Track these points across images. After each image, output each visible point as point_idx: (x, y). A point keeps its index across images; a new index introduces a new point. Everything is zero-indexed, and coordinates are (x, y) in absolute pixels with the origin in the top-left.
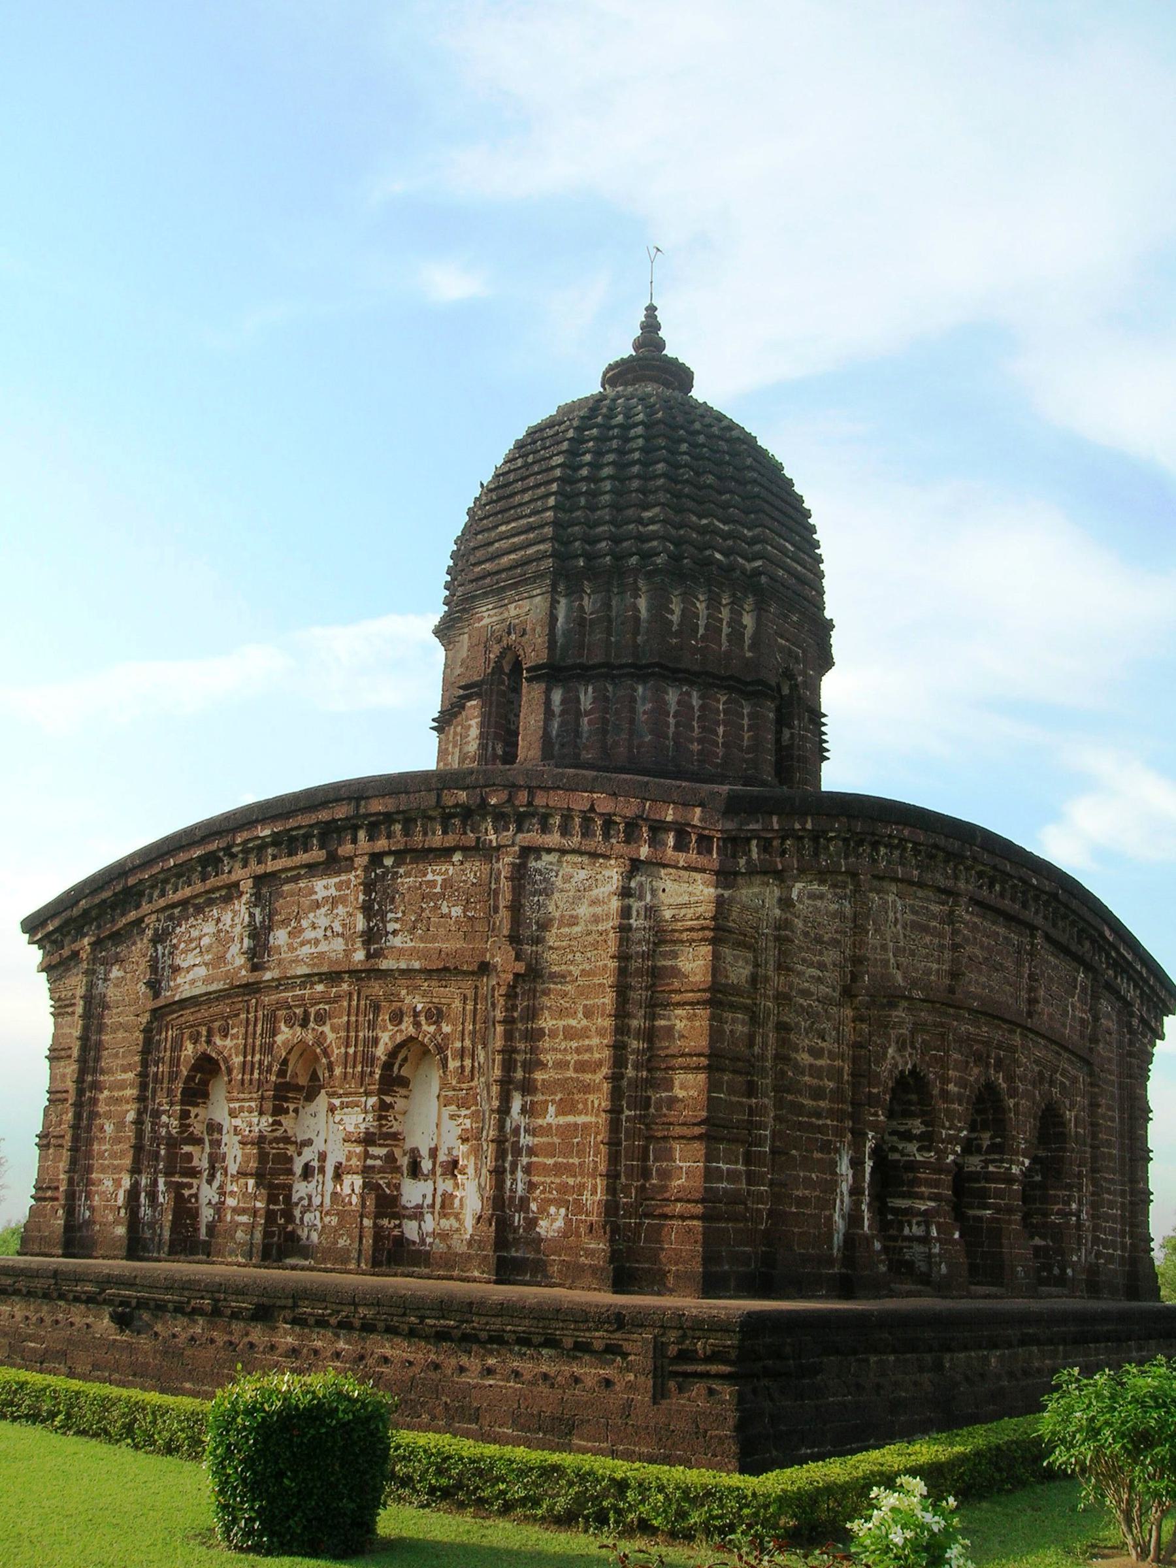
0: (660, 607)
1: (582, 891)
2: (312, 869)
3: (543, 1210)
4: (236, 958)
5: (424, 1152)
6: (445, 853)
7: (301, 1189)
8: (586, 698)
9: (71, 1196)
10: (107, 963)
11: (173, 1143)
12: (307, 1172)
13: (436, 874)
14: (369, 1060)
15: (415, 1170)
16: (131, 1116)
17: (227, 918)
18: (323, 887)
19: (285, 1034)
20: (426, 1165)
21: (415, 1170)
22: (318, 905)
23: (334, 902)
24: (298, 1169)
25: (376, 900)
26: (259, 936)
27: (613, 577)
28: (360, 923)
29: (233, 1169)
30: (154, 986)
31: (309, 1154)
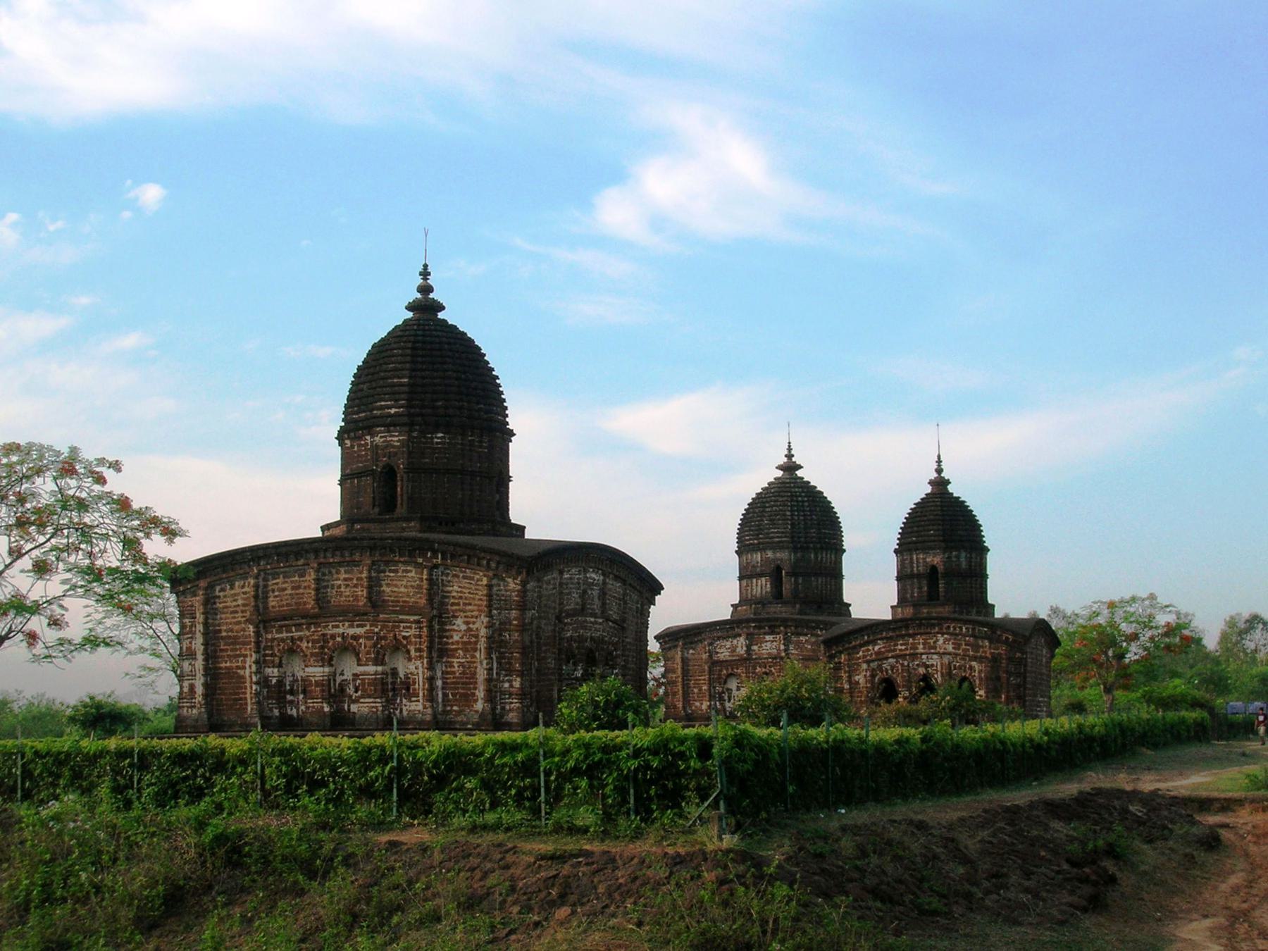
0: (816, 557)
4: (741, 651)
8: (800, 580)
9: (684, 708)
10: (688, 649)
11: (720, 694)
13: (803, 638)
16: (705, 687)
18: (768, 638)
19: (758, 669)
25: (787, 642)
26: (748, 647)
27: (805, 549)
28: (782, 647)
30: (710, 656)
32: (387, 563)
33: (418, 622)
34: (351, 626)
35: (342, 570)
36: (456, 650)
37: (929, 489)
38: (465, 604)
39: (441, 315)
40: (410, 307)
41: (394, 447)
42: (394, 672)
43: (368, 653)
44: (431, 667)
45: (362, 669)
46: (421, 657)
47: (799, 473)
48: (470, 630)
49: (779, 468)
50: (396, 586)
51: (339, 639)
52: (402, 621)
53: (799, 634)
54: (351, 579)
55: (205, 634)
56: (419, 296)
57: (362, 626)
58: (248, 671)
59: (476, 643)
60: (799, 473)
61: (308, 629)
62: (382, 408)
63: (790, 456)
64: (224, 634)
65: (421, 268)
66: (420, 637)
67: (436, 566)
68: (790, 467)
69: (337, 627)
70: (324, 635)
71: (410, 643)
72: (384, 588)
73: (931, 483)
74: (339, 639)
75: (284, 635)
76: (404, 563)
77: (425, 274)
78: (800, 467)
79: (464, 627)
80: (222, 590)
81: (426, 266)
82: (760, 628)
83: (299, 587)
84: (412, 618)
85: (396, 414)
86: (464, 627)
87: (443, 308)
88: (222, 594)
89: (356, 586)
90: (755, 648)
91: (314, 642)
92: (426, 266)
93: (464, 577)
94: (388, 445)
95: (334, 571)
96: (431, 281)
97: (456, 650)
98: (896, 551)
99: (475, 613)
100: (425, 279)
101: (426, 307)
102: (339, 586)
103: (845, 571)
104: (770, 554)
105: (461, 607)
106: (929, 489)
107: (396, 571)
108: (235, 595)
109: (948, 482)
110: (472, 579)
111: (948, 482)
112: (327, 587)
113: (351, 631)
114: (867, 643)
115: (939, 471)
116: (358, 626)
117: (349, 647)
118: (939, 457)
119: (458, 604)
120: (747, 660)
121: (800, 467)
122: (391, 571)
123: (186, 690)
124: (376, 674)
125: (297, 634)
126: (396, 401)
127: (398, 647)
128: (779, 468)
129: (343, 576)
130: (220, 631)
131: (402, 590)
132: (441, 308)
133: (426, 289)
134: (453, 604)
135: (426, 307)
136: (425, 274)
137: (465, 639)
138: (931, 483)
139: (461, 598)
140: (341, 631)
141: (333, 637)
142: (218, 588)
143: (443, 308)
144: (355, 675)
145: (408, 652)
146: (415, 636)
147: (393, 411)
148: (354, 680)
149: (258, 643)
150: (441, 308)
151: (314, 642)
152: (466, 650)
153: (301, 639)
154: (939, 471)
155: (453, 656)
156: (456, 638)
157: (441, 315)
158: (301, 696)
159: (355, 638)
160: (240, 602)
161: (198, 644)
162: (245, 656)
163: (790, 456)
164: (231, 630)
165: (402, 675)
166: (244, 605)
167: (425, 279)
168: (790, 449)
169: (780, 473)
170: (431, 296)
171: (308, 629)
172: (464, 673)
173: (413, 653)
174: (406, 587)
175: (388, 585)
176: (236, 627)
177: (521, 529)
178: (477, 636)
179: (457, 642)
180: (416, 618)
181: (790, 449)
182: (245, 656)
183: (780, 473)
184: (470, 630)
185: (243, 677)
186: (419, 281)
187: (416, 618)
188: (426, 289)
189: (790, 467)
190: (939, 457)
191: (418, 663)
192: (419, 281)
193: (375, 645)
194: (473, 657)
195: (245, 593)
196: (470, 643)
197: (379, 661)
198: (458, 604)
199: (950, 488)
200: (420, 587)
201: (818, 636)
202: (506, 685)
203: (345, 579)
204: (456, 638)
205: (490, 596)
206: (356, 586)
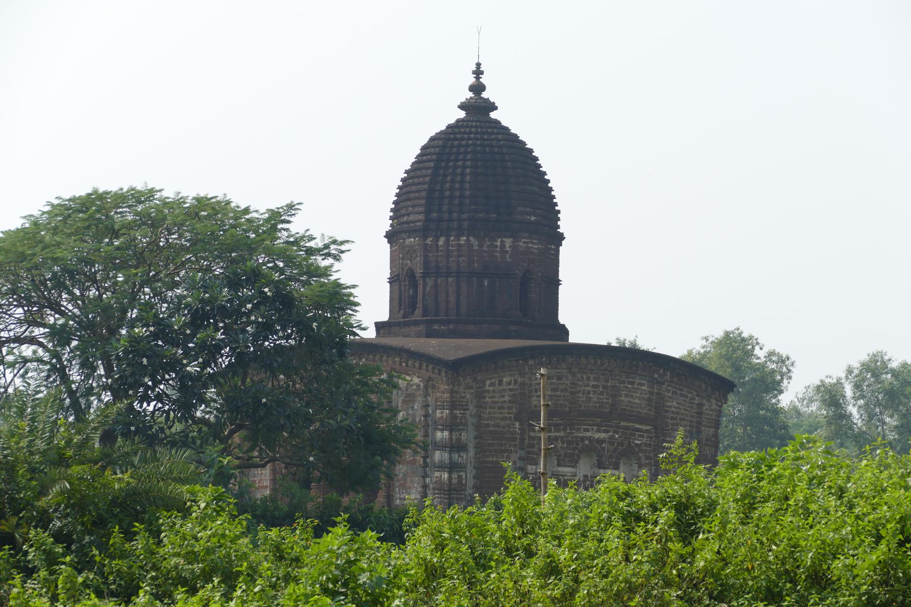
34: (598, 431)
35: (592, 376)
38: (681, 419)
39: (493, 115)
40: (462, 107)
43: (610, 457)
46: (650, 464)
50: (632, 397)
54: (597, 386)
55: (478, 427)
56: (471, 95)
57: (606, 431)
64: (492, 429)
65: (474, 68)
66: (650, 445)
69: (588, 430)
70: (576, 437)
74: (587, 442)
77: (478, 73)
80: (491, 385)
81: (478, 65)
83: (556, 390)
84: (644, 427)
87: (496, 108)
88: (491, 388)
89: (601, 393)
91: (569, 443)
92: (478, 65)
93: (681, 395)
95: (585, 377)
100: (478, 78)
101: (478, 107)
102: (589, 392)
107: (632, 383)
108: (504, 390)
112: (579, 392)
113: (598, 436)
119: (675, 419)
122: (630, 383)
123: (454, 481)
129: (592, 383)
130: (488, 426)
131: (637, 401)
133: (478, 88)
134: (672, 418)
135: (478, 107)
136: (478, 73)
139: (678, 413)
140: (589, 434)
141: (583, 439)
142: (488, 382)
143: (496, 108)
145: (639, 459)
146: (646, 445)
147: (533, 218)
149: (522, 439)
151: (569, 443)
157: (493, 115)
160: (507, 398)
161: (467, 436)
162: (511, 452)
164: (498, 426)
166: (510, 402)
167: (478, 78)
173: (643, 460)
174: (639, 399)
175: (626, 396)
176: (502, 423)
180: (648, 428)
182: (511, 452)
187: (648, 428)
188: (478, 88)
192: (472, 80)
195: (511, 390)
198: (675, 419)
200: (649, 400)
203: (594, 386)
206: (601, 393)
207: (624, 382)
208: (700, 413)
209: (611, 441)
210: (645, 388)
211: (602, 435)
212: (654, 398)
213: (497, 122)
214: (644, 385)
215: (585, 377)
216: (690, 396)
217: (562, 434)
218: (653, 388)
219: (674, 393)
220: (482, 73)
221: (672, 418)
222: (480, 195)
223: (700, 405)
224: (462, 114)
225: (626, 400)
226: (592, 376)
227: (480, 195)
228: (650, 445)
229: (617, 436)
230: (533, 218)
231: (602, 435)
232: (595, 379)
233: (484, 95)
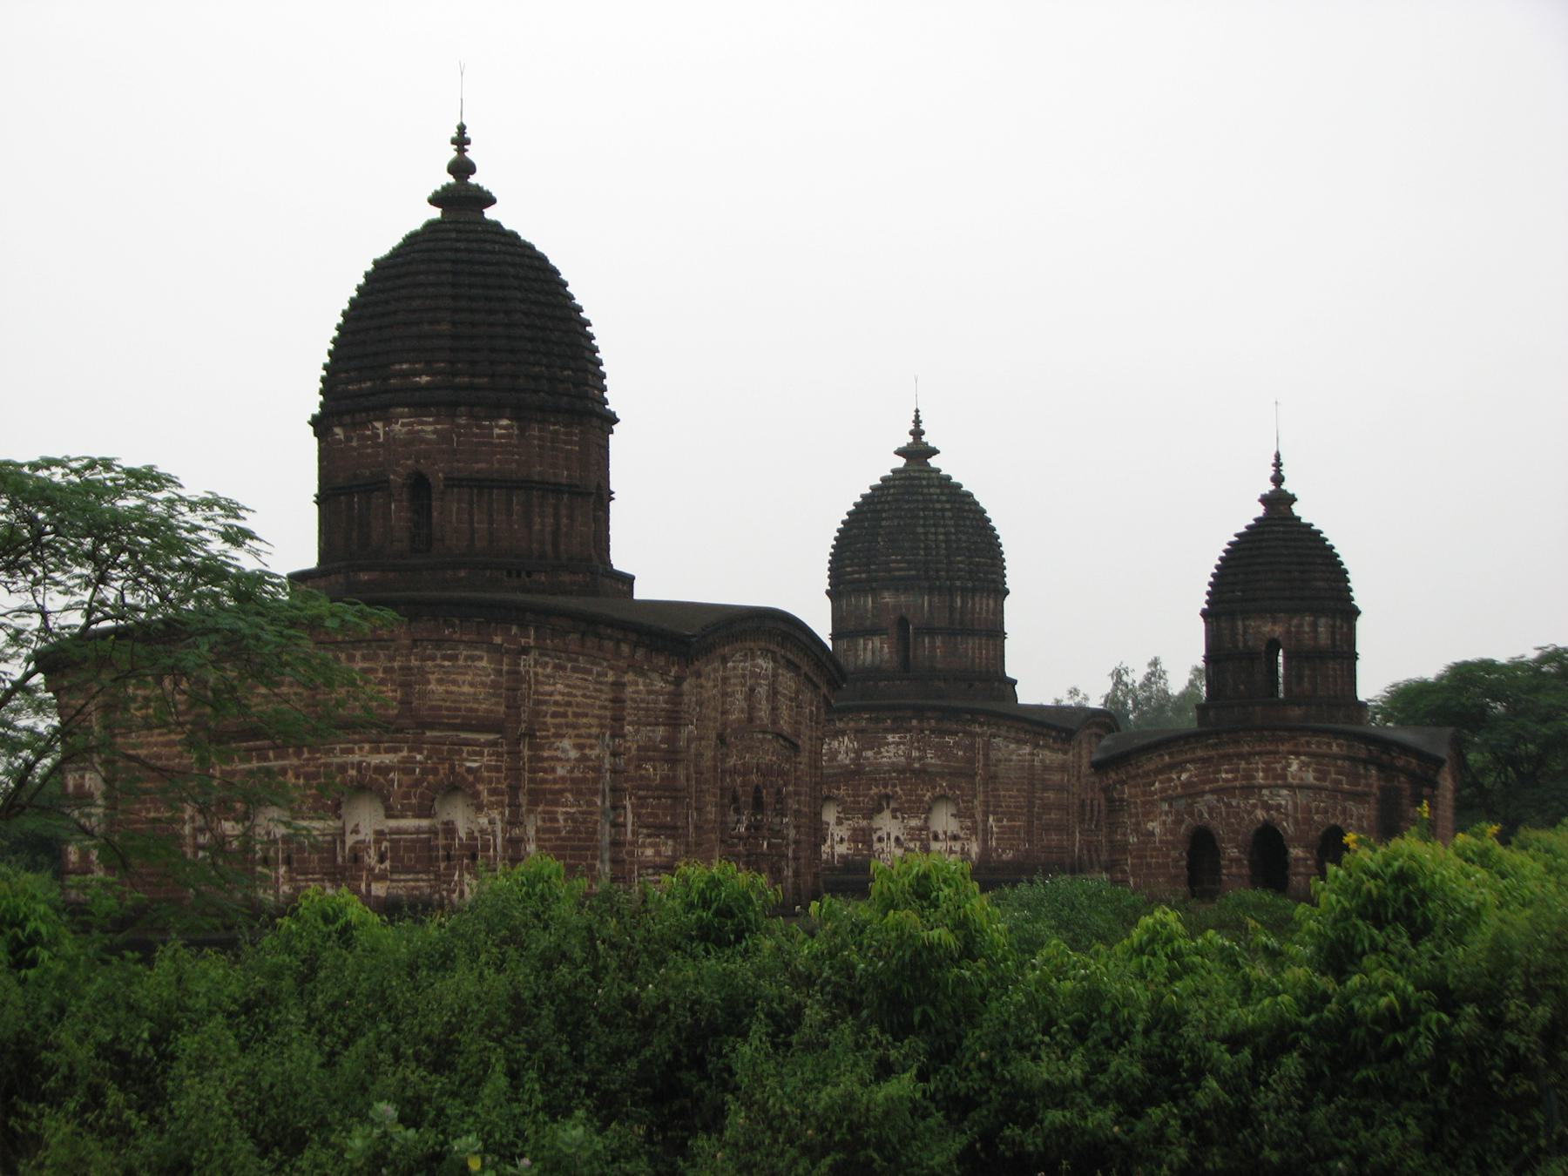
1: (1012, 753)
2: (887, 731)
3: (1004, 851)
5: (940, 832)
6: (956, 733)
7: (877, 846)
12: (880, 840)
13: (949, 740)
14: (921, 801)
15: (936, 838)
17: (836, 744)
18: (890, 738)
19: (874, 791)
20: (941, 836)
21: (936, 838)
22: (888, 744)
23: (898, 744)
24: (875, 837)
26: (858, 752)
29: (837, 839)
31: (879, 833)
32: (439, 643)
33: (494, 744)
35: (358, 654)
36: (561, 792)
37: (1260, 511)
38: (576, 715)
39: (490, 213)
40: (435, 200)
41: (428, 442)
42: (450, 829)
43: (406, 796)
44: (514, 821)
45: (393, 823)
46: (500, 804)
47: (933, 462)
48: (584, 758)
49: (900, 452)
50: (454, 682)
51: (353, 772)
52: (467, 743)
53: (943, 733)
56: (451, 179)
57: (395, 750)
58: (187, 829)
59: (596, 781)
60: (933, 462)
61: (298, 754)
62: (404, 375)
63: (917, 433)
65: (454, 133)
66: (497, 769)
67: (525, 650)
68: (918, 452)
69: (351, 751)
70: (326, 765)
71: (479, 780)
72: (432, 687)
73: (1264, 500)
74: (353, 772)
75: (255, 764)
76: (471, 644)
77: (461, 141)
78: (935, 452)
79: (573, 754)
81: (462, 129)
82: (877, 720)
84: (483, 737)
85: (426, 387)
86: (573, 754)
89: (382, 682)
90: (869, 754)
91: (308, 777)
92: (462, 129)
93: (574, 670)
94: (414, 438)
95: (343, 656)
96: (472, 154)
97: (561, 792)
98: (1204, 614)
99: (594, 731)
101: (462, 199)
103: (1009, 626)
104: (888, 598)
105: (571, 719)
106: (1260, 511)
107: (454, 658)
109: (1293, 499)
110: (589, 672)
111: (1293, 499)
113: (375, 760)
114: (1170, 767)
115: (1278, 479)
116: (387, 751)
117: (366, 786)
118: (1278, 457)
119: (565, 715)
120: (854, 774)
121: (935, 452)
122: (445, 658)
124: (418, 831)
125: (275, 764)
126: (428, 363)
127: (455, 787)
128: (900, 452)
131: (466, 689)
132: (490, 200)
133: (462, 168)
134: (554, 715)
135: (462, 199)
136: (461, 141)
137: (577, 774)
138: (1264, 500)
139: (569, 704)
140: (356, 758)
141: (342, 768)
144: (380, 834)
146: (489, 768)
147: (425, 379)
148: (378, 842)
150: (490, 200)
151: (308, 777)
152: (578, 793)
153: (283, 771)
154: (1278, 479)
155: (556, 803)
156: (560, 772)
157: (490, 213)
158: (282, 870)
159: (382, 770)
163: (917, 433)
165: (462, 833)
168: (917, 422)
169: (901, 462)
170: (473, 180)
171: (298, 754)
172: (575, 831)
174: (472, 685)
175: (440, 681)
177: (629, 580)
178: (597, 770)
179: (563, 779)
181: (917, 422)
183: (901, 462)
184: (584, 758)
185: (183, 837)
186: (451, 153)
187: (491, 737)
188: (462, 168)
189: (918, 452)
190: (1278, 457)
191: (495, 814)
193: (417, 783)
194: (590, 803)
196: (584, 780)
197: (425, 811)
199: (1297, 509)
200: (495, 685)
201: (972, 735)
202: (649, 852)
204: (560, 772)
205: (617, 701)
206: (382, 682)
207: (433, 658)
208: (617, 701)
209: (406, 768)
210: (484, 663)
211: (387, 759)
212: (503, 680)
213: (497, 225)
214: (480, 658)
215: (343, 656)
216: (596, 669)
217: (295, 762)
218: (500, 662)
219: (556, 667)
220: (468, 142)
221: (554, 715)
222: (466, 350)
223: (618, 685)
224: (436, 213)
225: (441, 689)
226: (358, 654)
227: (466, 350)
228: (497, 769)
229: (419, 757)
230: (425, 379)
231: (387, 759)
232: (364, 658)
233: (473, 180)
